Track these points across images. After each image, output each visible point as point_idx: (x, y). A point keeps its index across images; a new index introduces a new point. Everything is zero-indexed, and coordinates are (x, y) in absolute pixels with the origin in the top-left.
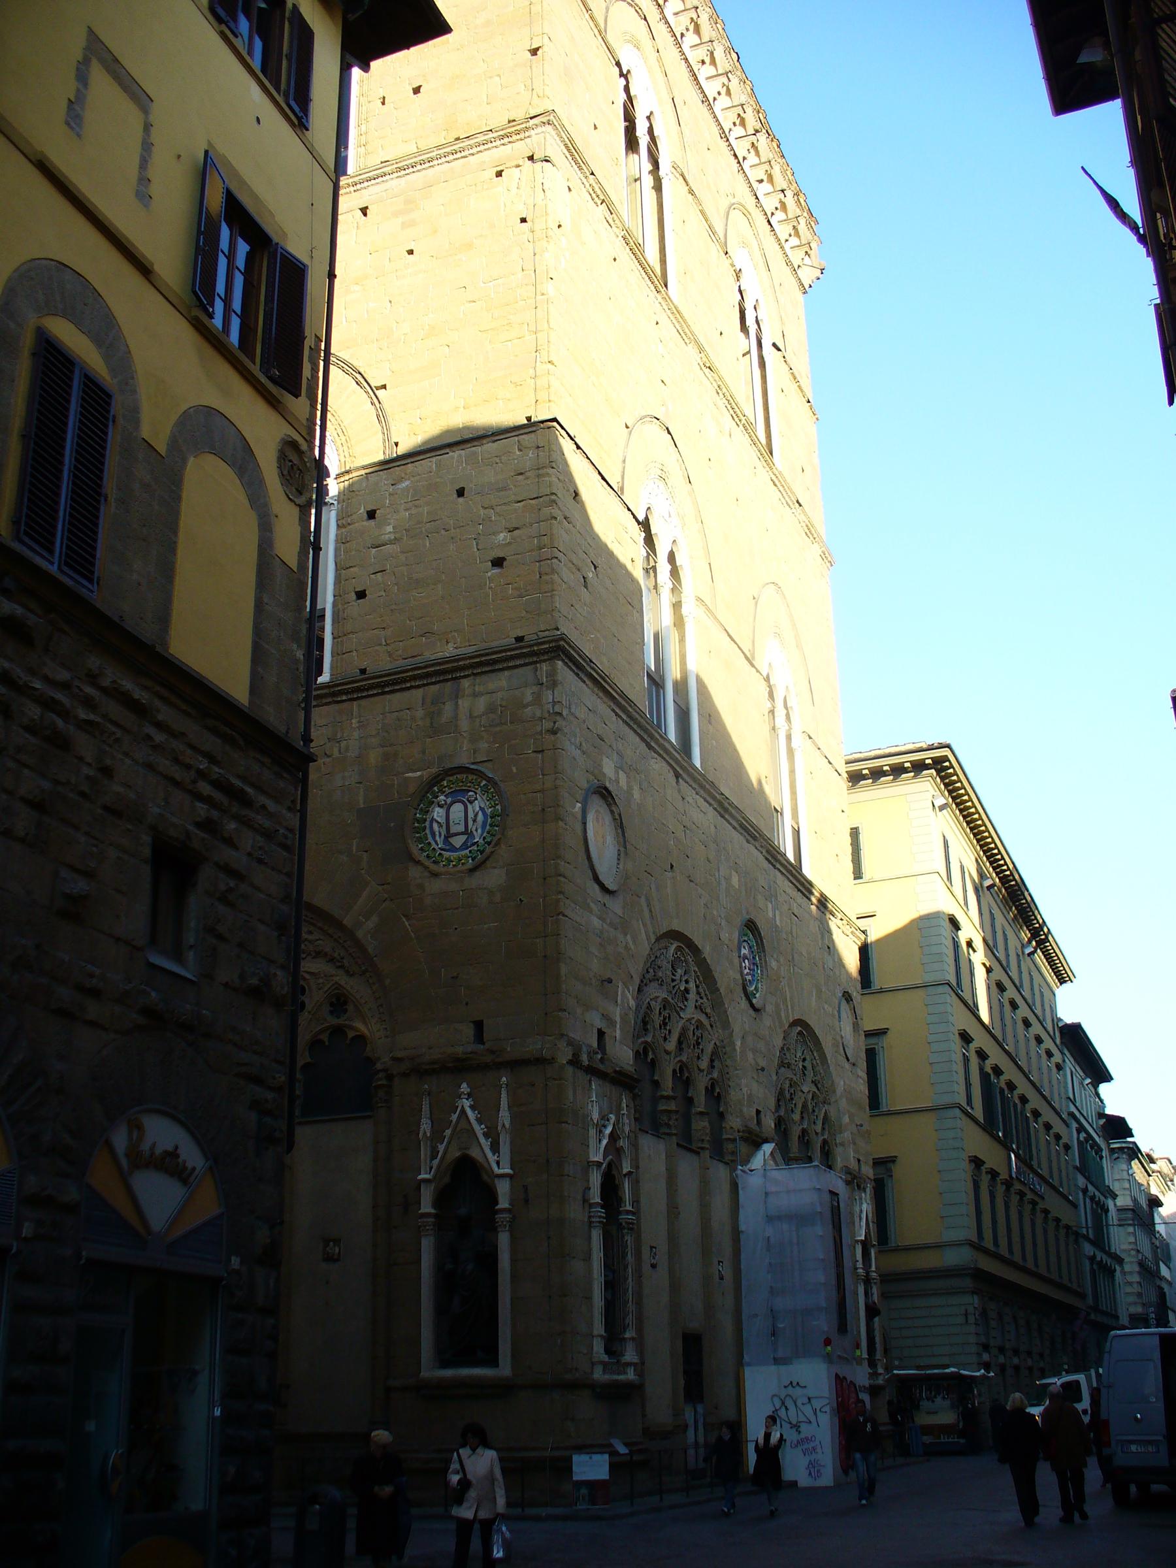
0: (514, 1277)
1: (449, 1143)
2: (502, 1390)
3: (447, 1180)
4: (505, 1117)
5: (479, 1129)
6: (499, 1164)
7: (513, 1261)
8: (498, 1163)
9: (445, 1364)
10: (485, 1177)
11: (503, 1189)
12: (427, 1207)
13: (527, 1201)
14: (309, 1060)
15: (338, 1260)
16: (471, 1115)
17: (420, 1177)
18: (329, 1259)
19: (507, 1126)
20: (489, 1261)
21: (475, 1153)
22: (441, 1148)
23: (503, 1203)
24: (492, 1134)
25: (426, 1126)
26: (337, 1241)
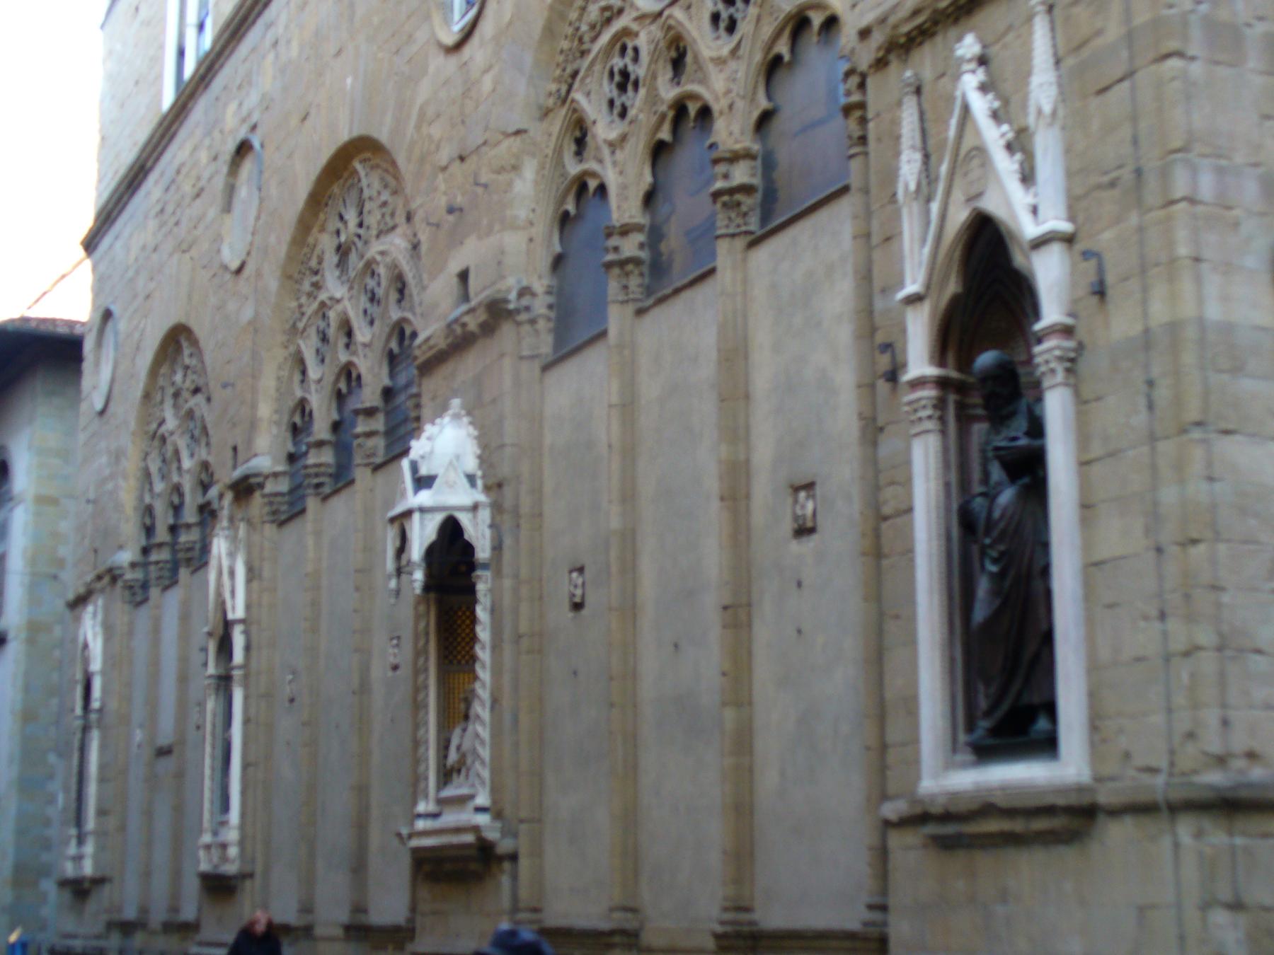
0: (1086, 507)
1: (948, 193)
2: (1073, 819)
3: (953, 287)
4: (1043, 88)
5: (993, 136)
6: (1030, 210)
7: (1084, 464)
8: (1034, 210)
9: (985, 752)
10: (1018, 260)
11: (1050, 275)
12: (919, 362)
13: (1100, 291)
14: (763, 103)
15: (812, 531)
16: (980, 105)
17: (901, 295)
18: (804, 530)
19: (1047, 109)
20: (1029, 468)
21: (991, 205)
22: (935, 207)
23: (1051, 312)
24: (1019, 144)
25: (909, 168)
26: (809, 486)
